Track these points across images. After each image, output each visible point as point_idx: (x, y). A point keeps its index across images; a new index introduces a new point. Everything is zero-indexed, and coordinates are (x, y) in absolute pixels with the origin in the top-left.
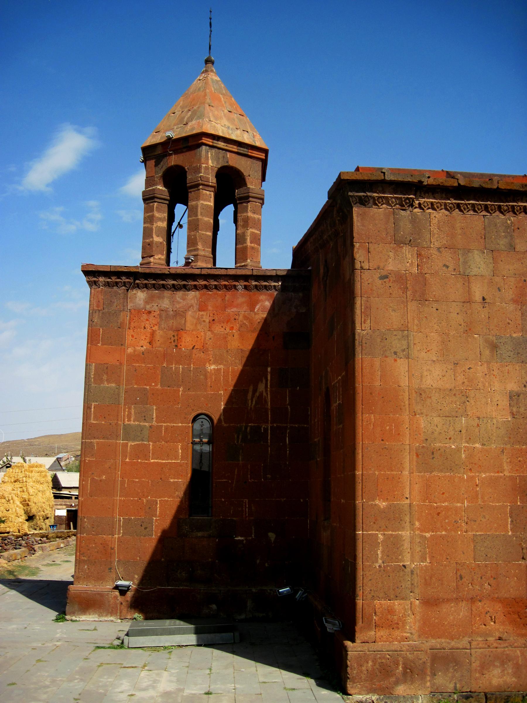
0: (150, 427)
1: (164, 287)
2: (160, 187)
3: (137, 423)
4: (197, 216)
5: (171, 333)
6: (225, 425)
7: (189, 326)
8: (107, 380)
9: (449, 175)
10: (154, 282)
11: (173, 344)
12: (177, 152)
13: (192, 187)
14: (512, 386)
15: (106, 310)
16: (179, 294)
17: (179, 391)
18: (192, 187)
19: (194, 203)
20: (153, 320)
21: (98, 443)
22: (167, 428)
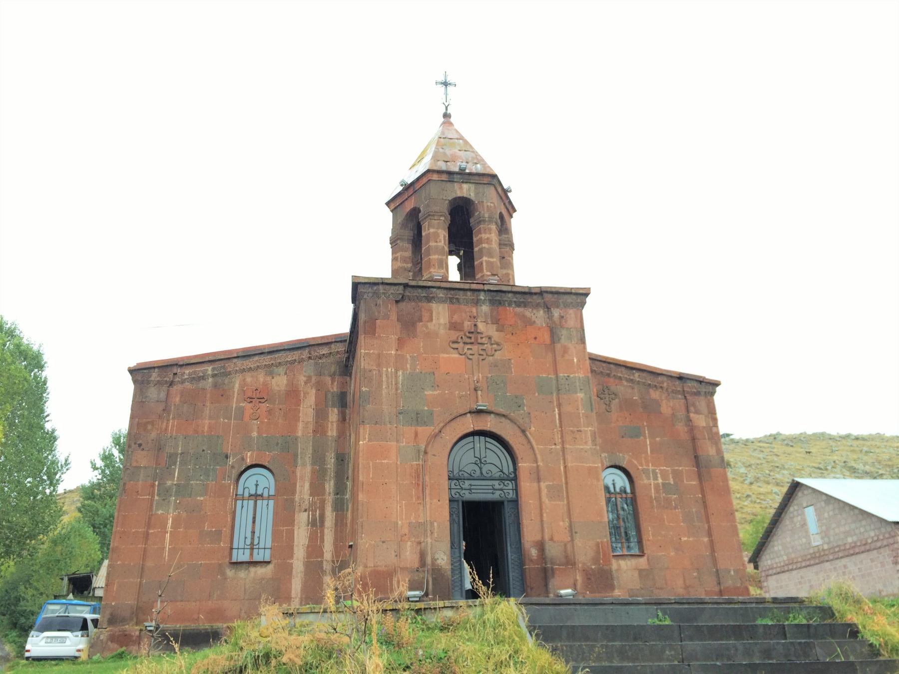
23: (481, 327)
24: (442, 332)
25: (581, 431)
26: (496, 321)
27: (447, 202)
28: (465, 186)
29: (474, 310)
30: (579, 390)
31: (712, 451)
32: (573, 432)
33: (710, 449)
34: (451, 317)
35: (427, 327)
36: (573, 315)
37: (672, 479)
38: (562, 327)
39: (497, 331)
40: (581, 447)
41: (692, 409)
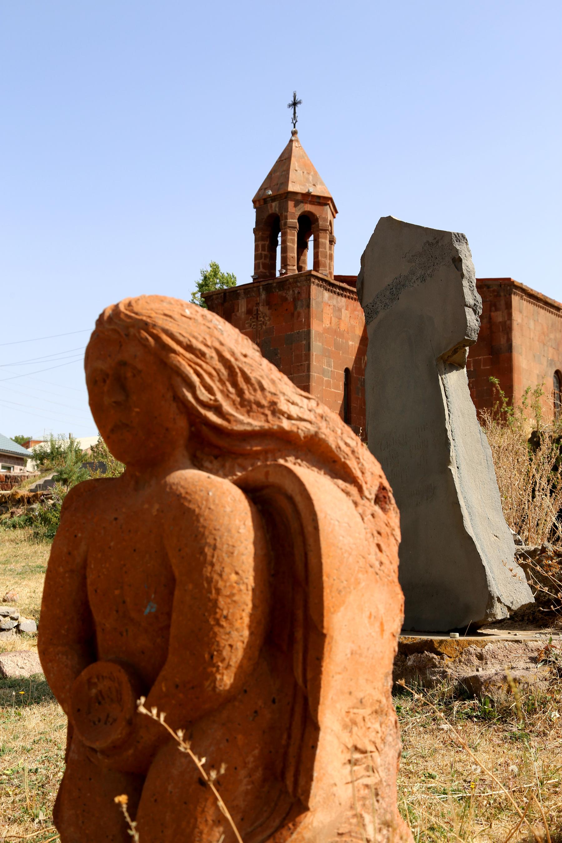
0: (331, 371)
1: (335, 292)
2: (296, 221)
3: (327, 368)
4: (326, 249)
5: (337, 320)
6: (355, 376)
7: (343, 318)
8: (319, 341)
9: (532, 290)
10: (332, 288)
11: (338, 326)
12: (312, 203)
13: (322, 230)
14: (538, 372)
15: (317, 300)
16: (340, 298)
17: (340, 353)
18: (322, 230)
19: (323, 240)
20: (332, 311)
21: (317, 376)
22: (337, 372)
23: (261, 308)
24: (243, 316)
25: (302, 365)
26: (268, 303)
27: (264, 220)
28: (274, 204)
29: (258, 299)
30: (303, 339)
31: (503, 341)
32: (298, 366)
33: (502, 339)
34: (247, 306)
35: (236, 315)
36: (305, 291)
37: (472, 367)
38: (298, 299)
39: (269, 309)
40: (301, 374)
41: (493, 308)
